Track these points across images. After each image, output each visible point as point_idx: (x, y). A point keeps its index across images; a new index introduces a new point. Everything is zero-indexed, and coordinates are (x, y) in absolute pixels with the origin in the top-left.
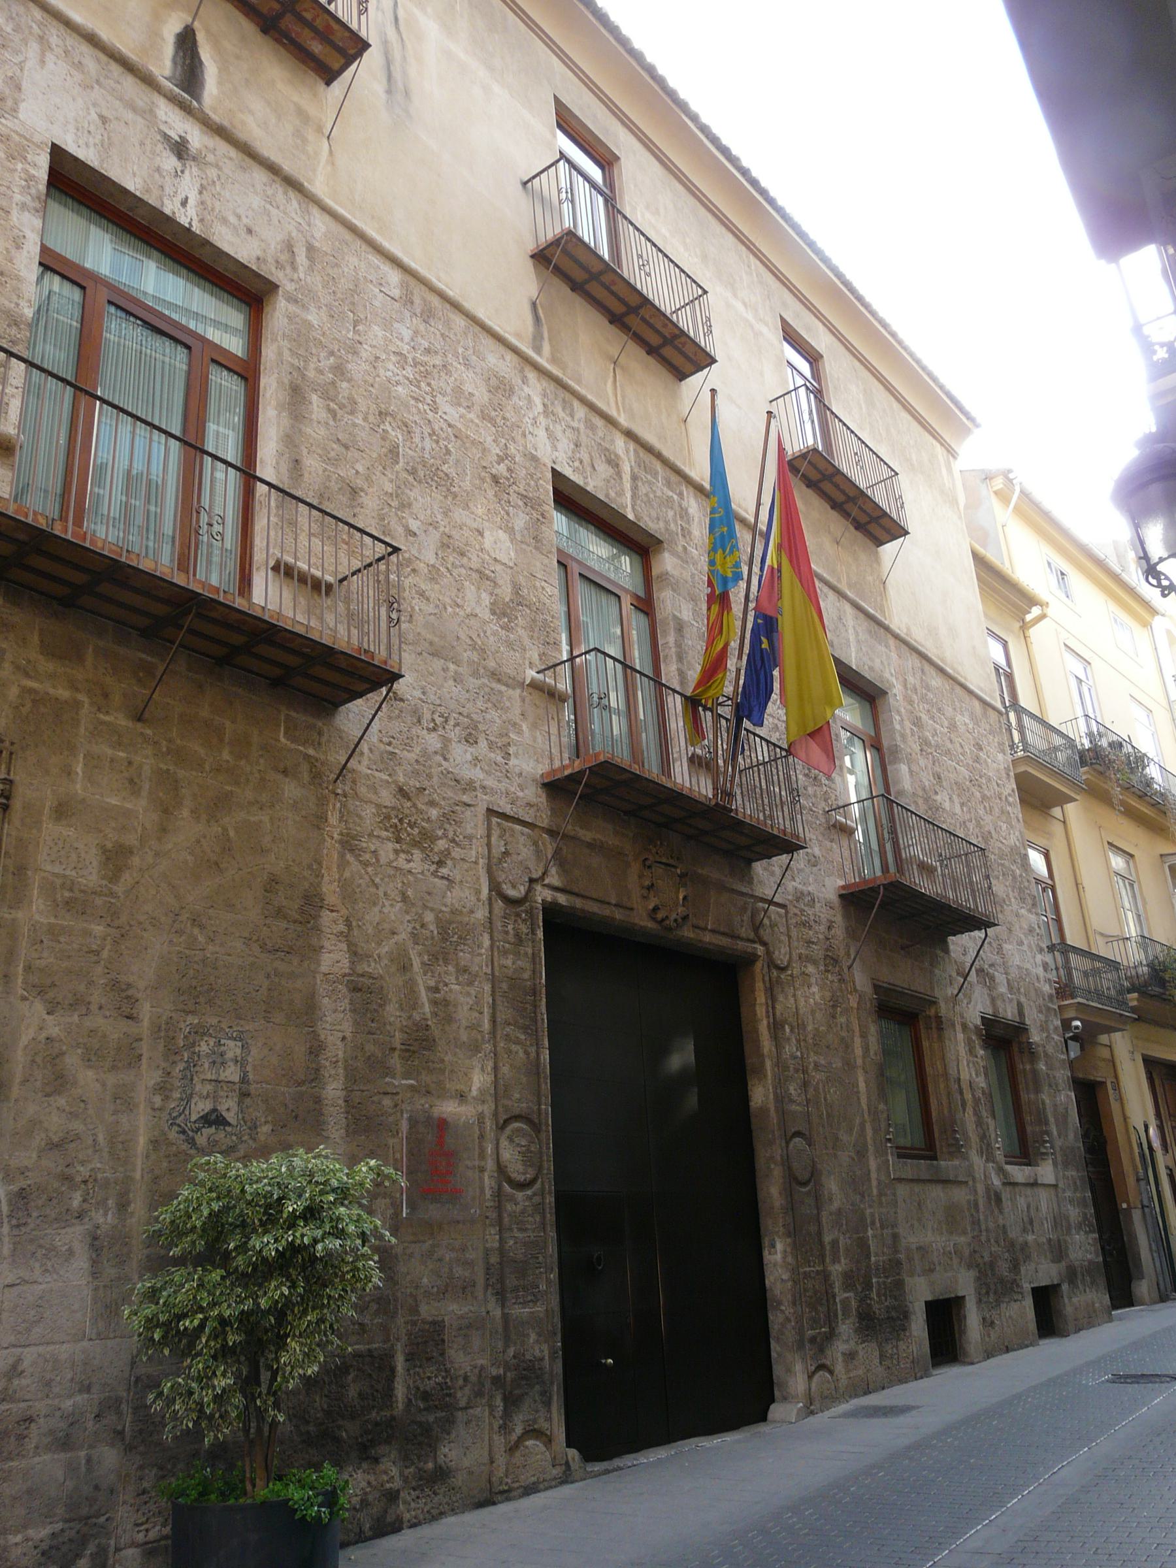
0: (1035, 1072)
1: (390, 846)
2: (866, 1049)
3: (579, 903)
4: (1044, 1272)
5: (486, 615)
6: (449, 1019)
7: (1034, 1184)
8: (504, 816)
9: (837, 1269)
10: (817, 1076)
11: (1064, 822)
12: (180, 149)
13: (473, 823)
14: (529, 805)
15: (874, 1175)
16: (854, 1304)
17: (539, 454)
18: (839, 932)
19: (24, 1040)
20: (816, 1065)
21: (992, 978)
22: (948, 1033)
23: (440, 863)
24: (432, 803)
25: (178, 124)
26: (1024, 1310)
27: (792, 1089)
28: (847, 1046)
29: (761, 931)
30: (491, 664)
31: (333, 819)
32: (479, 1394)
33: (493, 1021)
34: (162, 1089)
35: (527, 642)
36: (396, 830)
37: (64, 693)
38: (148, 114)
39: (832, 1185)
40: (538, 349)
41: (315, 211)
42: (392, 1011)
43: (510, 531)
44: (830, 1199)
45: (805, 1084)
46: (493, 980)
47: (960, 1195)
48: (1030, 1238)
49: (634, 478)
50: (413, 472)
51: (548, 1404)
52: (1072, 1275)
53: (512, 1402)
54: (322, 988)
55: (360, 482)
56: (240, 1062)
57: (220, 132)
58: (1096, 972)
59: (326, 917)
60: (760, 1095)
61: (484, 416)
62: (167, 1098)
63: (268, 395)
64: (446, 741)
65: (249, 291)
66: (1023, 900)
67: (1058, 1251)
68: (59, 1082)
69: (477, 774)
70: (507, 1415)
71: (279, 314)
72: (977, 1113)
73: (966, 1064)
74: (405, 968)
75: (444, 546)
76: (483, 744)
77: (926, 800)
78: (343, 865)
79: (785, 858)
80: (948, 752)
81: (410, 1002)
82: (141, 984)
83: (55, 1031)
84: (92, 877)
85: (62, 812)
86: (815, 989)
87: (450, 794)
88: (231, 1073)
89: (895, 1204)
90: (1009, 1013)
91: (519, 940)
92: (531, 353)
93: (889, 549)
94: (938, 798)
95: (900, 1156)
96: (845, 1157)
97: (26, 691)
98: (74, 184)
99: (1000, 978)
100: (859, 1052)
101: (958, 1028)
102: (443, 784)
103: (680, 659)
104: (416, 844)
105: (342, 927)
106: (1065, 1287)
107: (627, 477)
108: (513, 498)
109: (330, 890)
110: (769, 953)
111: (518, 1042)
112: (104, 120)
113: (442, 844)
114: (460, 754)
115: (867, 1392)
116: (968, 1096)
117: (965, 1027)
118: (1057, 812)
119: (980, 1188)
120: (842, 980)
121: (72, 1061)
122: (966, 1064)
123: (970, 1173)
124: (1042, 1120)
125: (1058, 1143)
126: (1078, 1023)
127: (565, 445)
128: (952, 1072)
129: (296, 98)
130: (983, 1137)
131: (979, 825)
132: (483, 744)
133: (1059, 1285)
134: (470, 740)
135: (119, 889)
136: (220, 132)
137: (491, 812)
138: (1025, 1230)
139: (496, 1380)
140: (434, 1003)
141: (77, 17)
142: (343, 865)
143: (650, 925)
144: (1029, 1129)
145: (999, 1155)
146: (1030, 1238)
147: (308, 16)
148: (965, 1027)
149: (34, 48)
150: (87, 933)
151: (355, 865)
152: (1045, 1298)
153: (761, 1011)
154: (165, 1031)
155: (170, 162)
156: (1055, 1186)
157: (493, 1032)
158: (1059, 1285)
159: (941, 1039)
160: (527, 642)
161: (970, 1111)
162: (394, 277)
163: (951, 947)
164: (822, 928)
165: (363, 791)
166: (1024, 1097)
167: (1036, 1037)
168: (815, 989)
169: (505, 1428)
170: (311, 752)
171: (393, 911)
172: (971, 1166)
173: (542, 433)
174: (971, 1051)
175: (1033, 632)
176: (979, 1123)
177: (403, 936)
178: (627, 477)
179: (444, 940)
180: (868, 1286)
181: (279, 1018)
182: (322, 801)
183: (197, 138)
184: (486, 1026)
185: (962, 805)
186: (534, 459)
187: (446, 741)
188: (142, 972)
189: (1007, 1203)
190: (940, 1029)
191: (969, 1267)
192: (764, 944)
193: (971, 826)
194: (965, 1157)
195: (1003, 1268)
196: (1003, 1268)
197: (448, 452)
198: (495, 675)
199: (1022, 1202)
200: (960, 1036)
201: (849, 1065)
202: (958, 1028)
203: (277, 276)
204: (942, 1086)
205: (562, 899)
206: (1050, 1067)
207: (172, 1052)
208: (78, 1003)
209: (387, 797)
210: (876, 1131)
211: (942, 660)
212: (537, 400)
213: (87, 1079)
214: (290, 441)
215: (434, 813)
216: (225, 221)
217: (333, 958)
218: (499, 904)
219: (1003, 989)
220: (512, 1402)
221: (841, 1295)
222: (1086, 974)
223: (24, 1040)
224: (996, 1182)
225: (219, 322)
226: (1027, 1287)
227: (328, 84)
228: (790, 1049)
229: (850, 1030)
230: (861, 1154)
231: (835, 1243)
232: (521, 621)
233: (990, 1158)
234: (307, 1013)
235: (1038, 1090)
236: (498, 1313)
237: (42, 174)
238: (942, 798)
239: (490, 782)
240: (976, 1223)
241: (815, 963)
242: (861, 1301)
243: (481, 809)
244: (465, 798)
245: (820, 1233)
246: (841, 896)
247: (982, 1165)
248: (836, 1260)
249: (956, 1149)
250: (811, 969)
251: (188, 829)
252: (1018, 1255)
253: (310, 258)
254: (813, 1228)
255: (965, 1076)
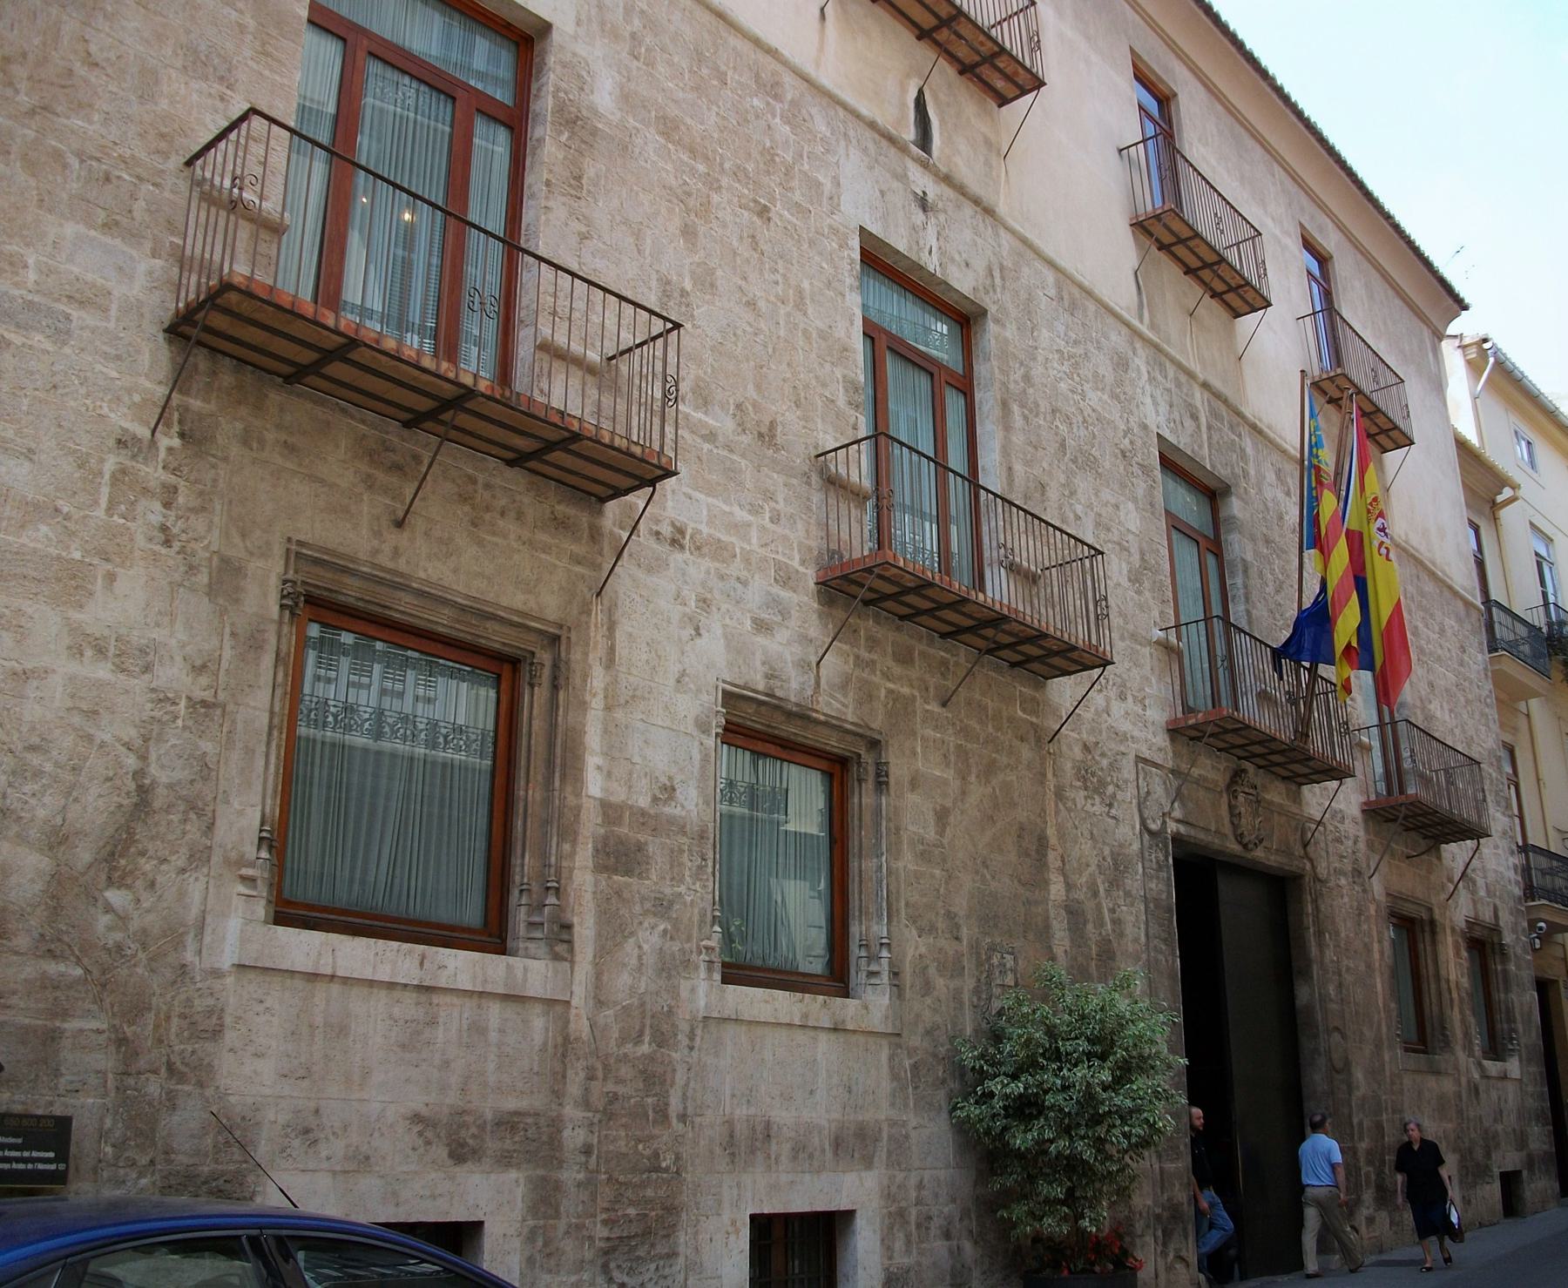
0: (1505, 972)
1: (1082, 793)
2: (1382, 953)
3: (1193, 832)
4: (1508, 1159)
5: (1126, 584)
6: (1121, 935)
7: (1504, 1077)
8: (1145, 761)
9: (1363, 1146)
10: (1348, 978)
11: (1528, 715)
12: (923, 203)
13: (1128, 770)
14: (1160, 750)
15: (1387, 1067)
16: (1373, 1177)
17: (1147, 422)
18: (1362, 845)
19: (909, 958)
20: (1348, 969)
21: (1474, 883)
22: (1440, 937)
23: (1110, 805)
24: (1103, 755)
25: (922, 181)
26: (1492, 1191)
27: (1332, 990)
28: (1369, 950)
29: (1310, 849)
30: (1131, 627)
31: (1050, 775)
32: (1148, 1226)
33: (1147, 935)
34: (976, 991)
35: (1151, 602)
36: (1085, 780)
37: (906, 690)
38: (902, 177)
39: (1359, 1075)
40: (1141, 320)
41: (1002, 232)
42: (1090, 927)
43: (1135, 500)
44: (1358, 1088)
45: (1340, 985)
46: (1145, 900)
47: (1448, 1085)
48: (1500, 1127)
49: (1209, 428)
50: (1074, 461)
51: (1186, 1238)
52: (1530, 1162)
53: (1167, 1234)
54: (1052, 913)
55: (1045, 479)
56: (1014, 971)
57: (947, 179)
58: (1551, 872)
59: (1051, 855)
60: (1303, 994)
61: (1114, 396)
62: (979, 998)
63: (985, 408)
64: (1108, 700)
65: (966, 320)
66: (1498, 803)
67: (1521, 1142)
68: (927, 987)
69: (1125, 726)
70: (1165, 1244)
71: (992, 336)
72: (1462, 1012)
73: (1454, 965)
74: (1095, 894)
75: (1098, 524)
76: (1130, 699)
77: (1423, 709)
78: (1057, 812)
79: (1335, 784)
80: (1439, 659)
81: (1100, 923)
82: (962, 913)
83: (923, 950)
84: (931, 834)
85: (914, 784)
86: (1346, 899)
87: (1113, 746)
88: (1009, 980)
89: (1401, 1092)
90: (1487, 916)
91: (1160, 868)
92: (1136, 322)
93: (1393, 458)
94: (1432, 707)
95: (1406, 1050)
96: (1368, 1049)
97: (890, 692)
98: (878, 261)
99: (1480, 882)
100: (1376, 956)
101: (1448, 931)
102: (1109, 738)
103: (1247, 599)
104: (1096, 791)
105: (1059, 863)
106: (1525, 1174)
107: (1204, 429)
108: (1136, 469)
109: (1051, 832)
110: (1314, 868)
111: (1161, 952)
112: (882, 193)
113: (1111, 789)
114: (1117, 708)
115: (1381, 1252)
116: (1455, 995)
117: (1453, 930)
118: (1522, 706)
119: (1464, 1080)
120: (1364, 891)
121: (932, 970)
122: (1454, 965)
123: (1456, 1068)
124: (1510, 1019)
125: (1523, 1041)
126: (1542, 924)
127: (1163, 408)
128: (1443, 973)
129: (983, 129)
130: (1466, 1034)
131: (1464, 731)
132: (1130, 699)
133: (1520, 1172)
134: (1122, 697)
135: (945, 841)
136: (947, 179)
137: (1140, 760)
138: (1495, 1120)
139: (1158, 1217)
140: (1114, 922)
141: (864, 111)
142: (1057, 812)
143: (1234, 847)
144: (1499, 1026)
145: (1477, 1051)
146: (1500, 1127)
147: (1001, 65)
148: (1453, 930)
149: (843, 143)
150: (933, 876)
151: (1064, 813)
152: (1510, 1181)
153: (1309, 921)
154: (975, 947)
155: (919, 217)
156: (1520, 1080)
157: (1147, 944)
158: (1520, 1172)
159: (1434, 942)
160: (1151, 602)
161: (1456, 1009)
162: (1050, 277)
163: (1444, 855)
164: (1350, 843)
165: (1064, 748)
166: (1495, 996)
167: (1508, 938)
168: (1346, 899)
169: (1164, 1254)
170: (1034, 720)
171: (1087, 846)
172: (1457, 1059)
173: (1148, 401)
174: (1458, 954)
175: (1505, 514)
176: (1463, 1021)
177: (1093, 868)
178: (1204, 429)
179: (1116, 869)
180: (1383, 1162)
181: (1031, 936)
182: (1043, 759)
183: (933, 190)
184: (1143, 939)
185: (1451, 711)
186: (1145, 427)
187: (1108, 700)
188: (961, 905)
189: (1483, 1096)
190: (1433, 933)
191: (1454, 1151)
192: (1311, 860)
193: (1457, 731)
194: (1453, 1052)
195: (1479, 1154)
196: (1479, 1154)
197: (1094, 437)
198: (1133, 636)
199: (1494, 1095)
200: (1450, 940)
201: (1369, 966)
202: (1448, 931)
203: (987, 302)
204: (1433, 986)
205: (1182, 829)
206: (1519, 968)
207: (979, 964)
208: (932, 929)
209: (1077, 752)
210: (1389, 1028)
211: (1434, 564)
212: (1144, 369)
213: (940, 983)
214: (1006, 451)
215: (1105, 763)
216: (953, 260)
217: (1057, 890)
218: (1146, 836)
219: (1482, 893)
220: (1167, 1234)
221: (1365, 1169)
222: (1544, 873)
223: (909, 958)
224: (1476, 1076)
225: (937, 338)
226: (1496, 1171)
227: (1000, 106)
228: (1330, 954)
229: (1370, 936)
230: (1378, 1046)
231: (1361, 1124)
232: (1146, 584)
233: (1471, 1054)
234: (1045, 932)
235: (1507, 990)
236: (1156, 1166)
237: (857, 256)
238: (1434, 707)
239: (1136, 733)
240: (1460, 1112)
241: (1345, 874)
242: (1378, 1175)
243: (1132, 757)
244: (1122, 749)
245: (1350, 1116)
246: (1363, 811)
247: (1465, 1059)
248: (1361, 1139)
249: (1447, 1045)
250: (1343, 881)
251: (977, 792)
252: (1490, 1142)
253: (1003, 278)
254: (1346, 1111)
255: (1453, 977)
